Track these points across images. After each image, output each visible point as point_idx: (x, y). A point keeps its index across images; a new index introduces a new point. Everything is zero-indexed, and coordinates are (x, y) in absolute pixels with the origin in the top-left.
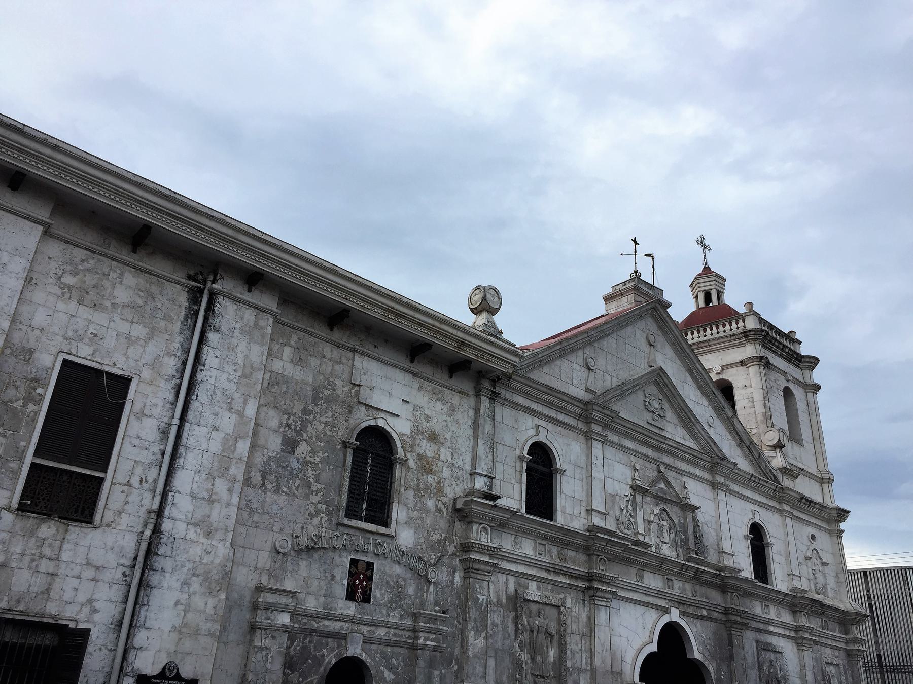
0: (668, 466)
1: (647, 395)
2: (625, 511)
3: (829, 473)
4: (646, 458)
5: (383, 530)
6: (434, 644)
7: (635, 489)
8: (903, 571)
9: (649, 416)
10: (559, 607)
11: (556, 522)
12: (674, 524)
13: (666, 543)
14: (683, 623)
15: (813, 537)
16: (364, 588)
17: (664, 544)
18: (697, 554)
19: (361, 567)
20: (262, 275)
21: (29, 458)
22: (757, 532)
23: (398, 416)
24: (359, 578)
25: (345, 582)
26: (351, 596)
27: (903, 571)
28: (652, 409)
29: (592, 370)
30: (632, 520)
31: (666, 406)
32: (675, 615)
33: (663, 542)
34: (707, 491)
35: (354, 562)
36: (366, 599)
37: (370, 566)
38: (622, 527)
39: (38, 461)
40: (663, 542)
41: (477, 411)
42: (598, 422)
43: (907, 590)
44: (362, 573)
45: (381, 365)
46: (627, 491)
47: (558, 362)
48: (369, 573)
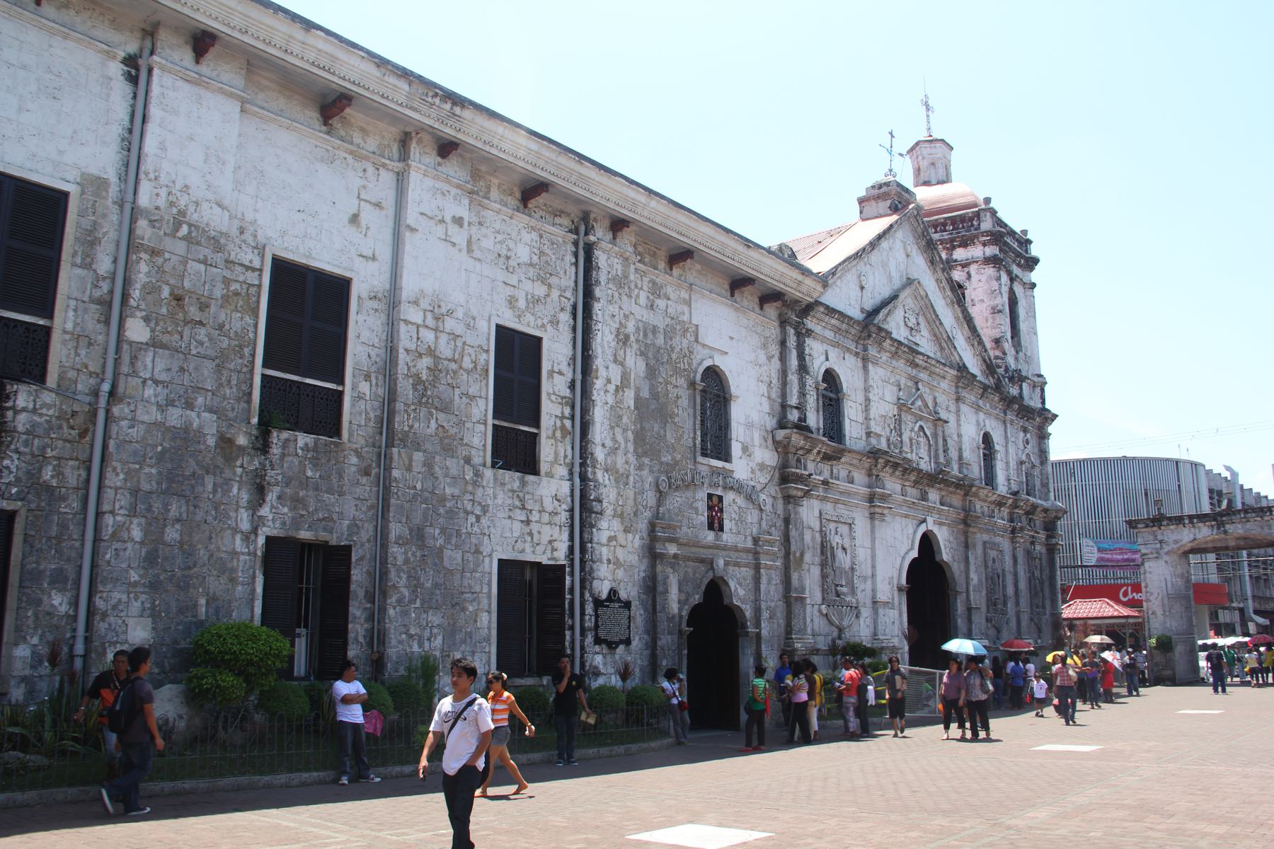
2: (893, 431)
3: (1040, 376)
5: (727, 465)
8: (1072, 464)
10: (850, 524)
11: (845, 445)
12: (929, 441)
16: (719, 518)
19: (715, 500)
20: (628, 222)
21: (490, 421)
22: (987, 439)
23: (726, 353)
24: (714, 510)
25: (706, 515)
26: (711, 527)
27: (1072, 464)
31: (921, 319)
35: (710, 496)
36: (721, 529)
37: (720, 498)
39: (497, 422)
41: (783, 343)
43: (1073, 483)
44: (715, 506)
48: (720, 505)
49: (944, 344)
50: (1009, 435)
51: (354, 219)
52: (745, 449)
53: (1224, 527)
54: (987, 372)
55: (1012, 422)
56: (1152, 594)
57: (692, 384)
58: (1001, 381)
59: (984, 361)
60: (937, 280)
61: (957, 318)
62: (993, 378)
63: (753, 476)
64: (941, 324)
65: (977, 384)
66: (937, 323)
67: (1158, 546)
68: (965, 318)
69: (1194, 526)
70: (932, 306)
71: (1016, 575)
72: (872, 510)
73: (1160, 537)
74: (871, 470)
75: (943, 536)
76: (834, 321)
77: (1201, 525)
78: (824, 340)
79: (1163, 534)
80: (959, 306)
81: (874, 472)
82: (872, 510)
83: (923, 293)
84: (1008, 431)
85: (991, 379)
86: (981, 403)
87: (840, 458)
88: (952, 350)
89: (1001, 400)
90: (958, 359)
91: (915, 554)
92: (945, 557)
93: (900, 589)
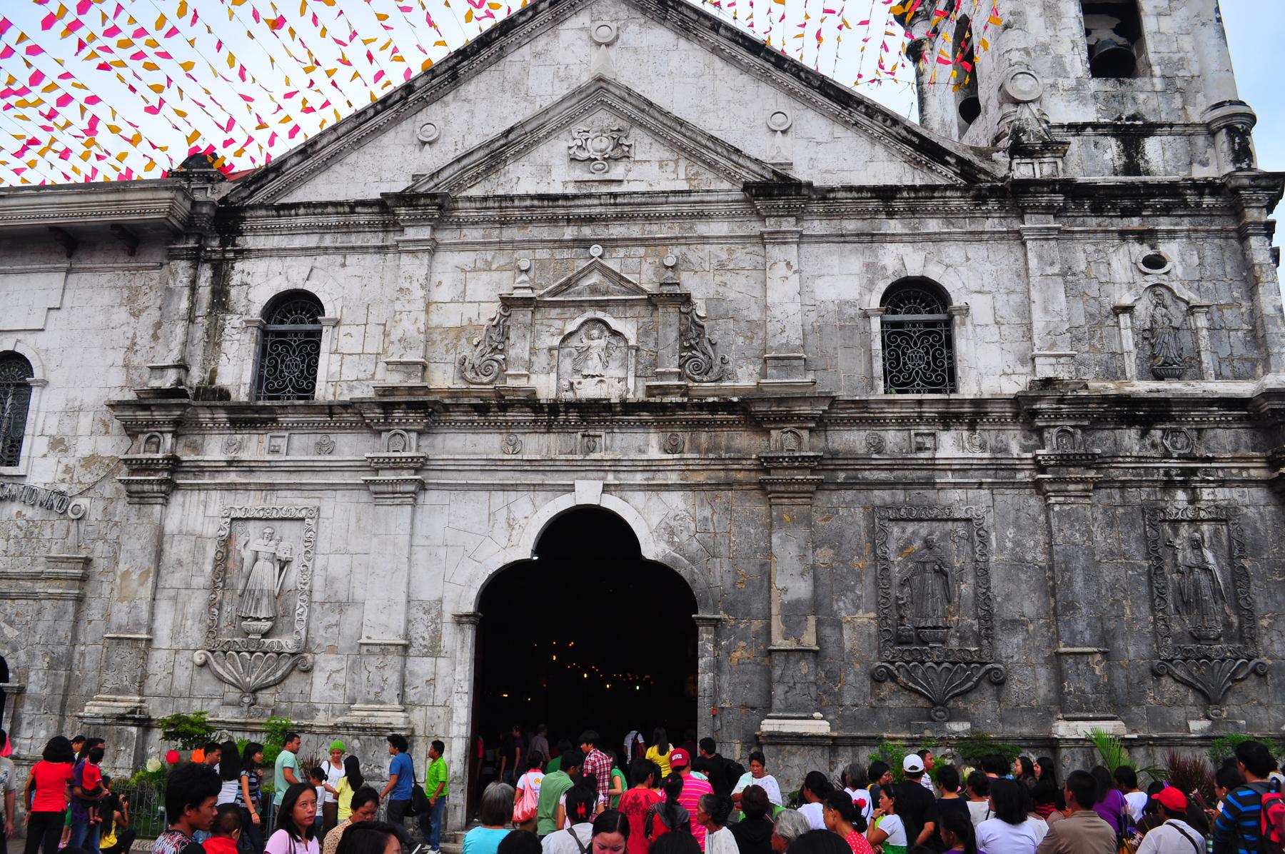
0: (609, 244)
1: (576, 135)
4: (562, 244)
6: (60, 591)
7: (508, 303)
9: (580, 173)
10: (303, 519)
12: (626, 341)
13: (593, 376)
14: (612, 503)
15: (1156, 262)
17: (589, 379)
18: (680, 376)
23: (43, 330)
28: (584, 155)
29: (430, 143)
30: (500, 357)
32: (588, 492)
33: (586, 377)
34: (743, 256)
38: (470, 375)
40: (586, 377)
42: (415, 222)
45: (20, 277)
46: (494, 309)
47: (353, 158)
50: (1033, 262)
54: (924, 158)
55: (1045, 235)
58: (969, 163)
59: (905, 141)
60: (715, 50)
61: (791, 93)
62: (946, 164)
63: (67, 477)
64: (682, 123)
65: (840, 195)
68: (809, 85)
70: (650, 104)
76: (300, 221)
78: (281, 253)
80: (785, 71)
83: (618, 92)
84: (1030, 255)
85: (940, 168)
86: (895, 226)
87: (275, 420)
88: (735, 157)
91: (524, 550)
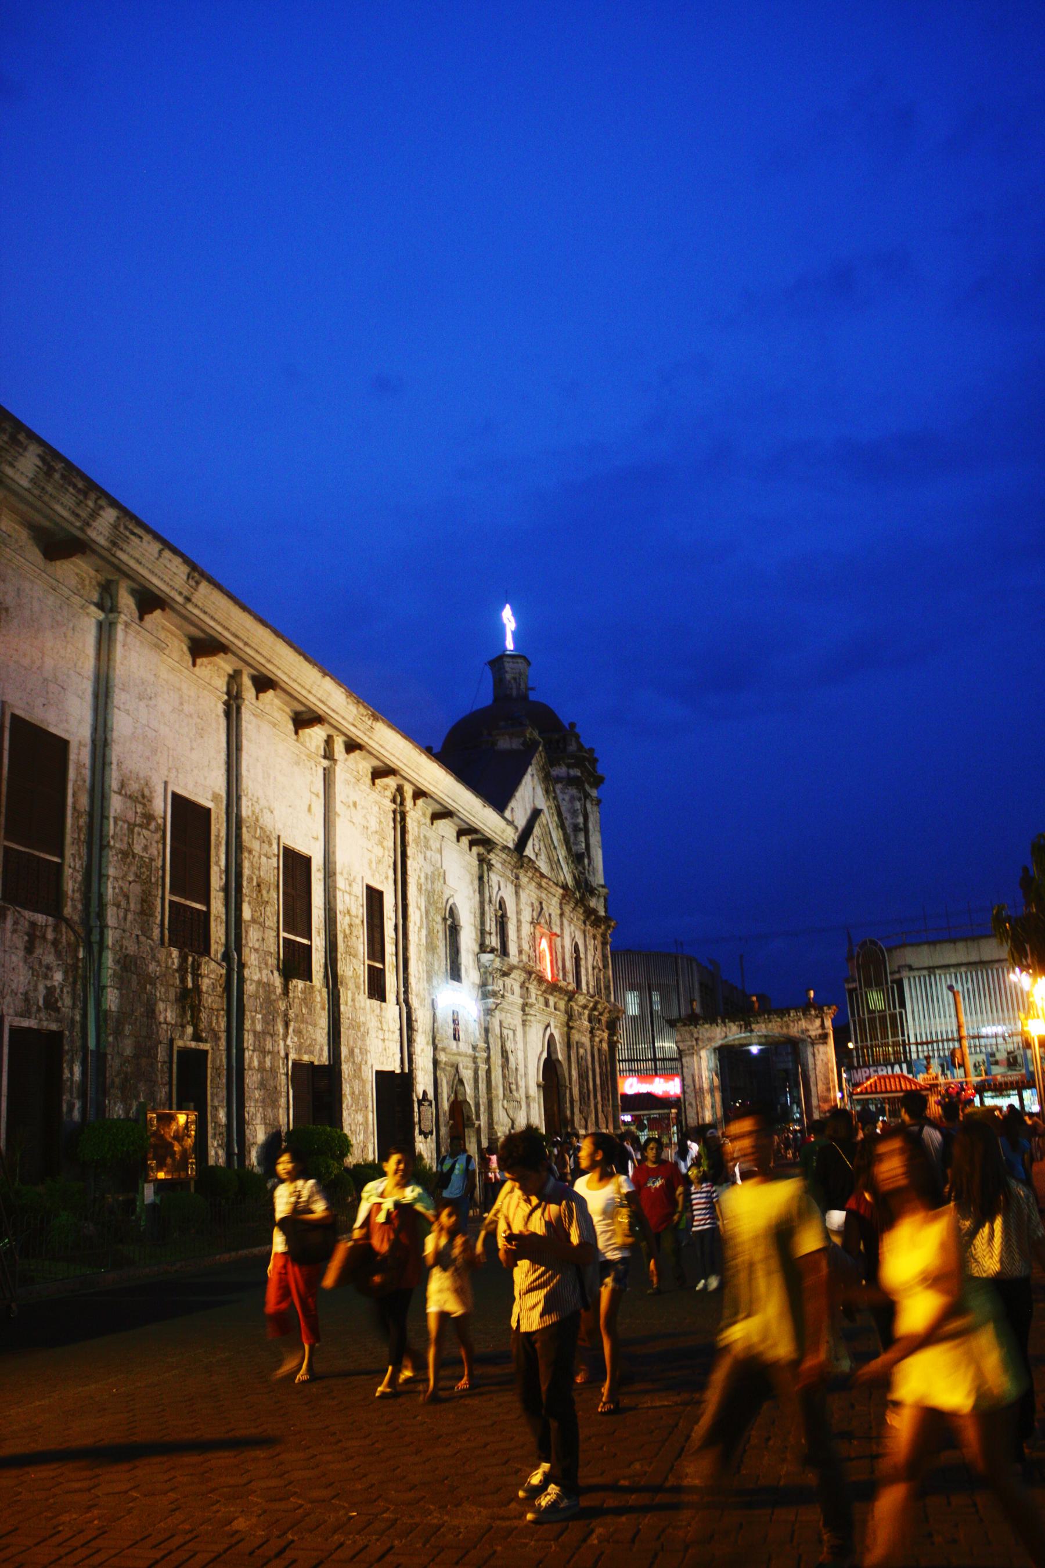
49: (554, 866)
51: (309, 809)
52: (466, 970)
53: (750, 1026)
56: (688, 1087)
57: (445, 919)
66: (552, 847)
67: (694, 1043)
69: (725, 1026)
71: (594, 1071)
72: (525, 1018)
73: (696, 1035)
74: (524, 982)
75: (557, 1037)
77: (732, 1024)
79: (698, 1032)
81: (527, 985)
82: (525, 1018)
89: (585, 912)
90: (562, 878)
92: (560, 1057)
93: (539, 1086)
